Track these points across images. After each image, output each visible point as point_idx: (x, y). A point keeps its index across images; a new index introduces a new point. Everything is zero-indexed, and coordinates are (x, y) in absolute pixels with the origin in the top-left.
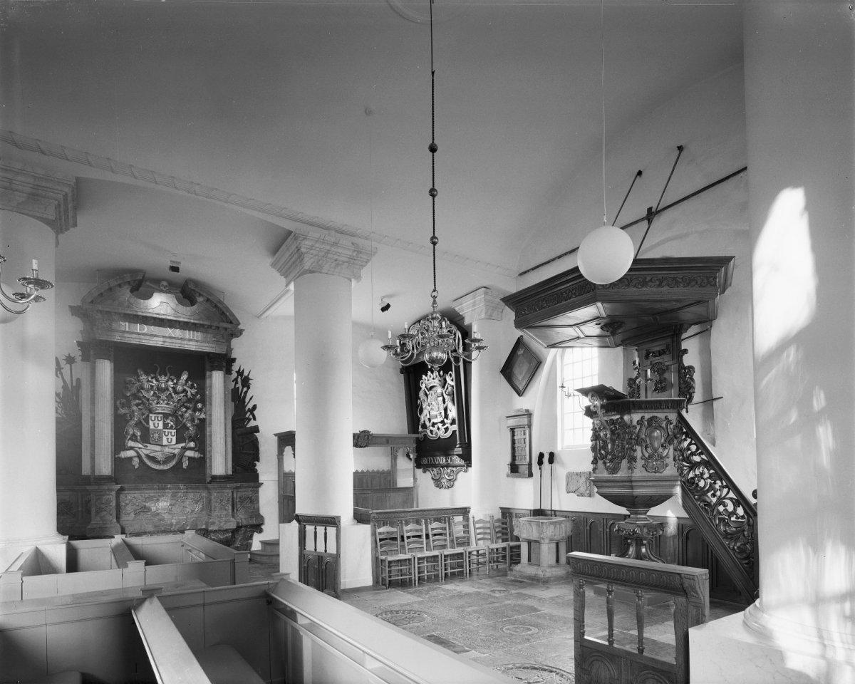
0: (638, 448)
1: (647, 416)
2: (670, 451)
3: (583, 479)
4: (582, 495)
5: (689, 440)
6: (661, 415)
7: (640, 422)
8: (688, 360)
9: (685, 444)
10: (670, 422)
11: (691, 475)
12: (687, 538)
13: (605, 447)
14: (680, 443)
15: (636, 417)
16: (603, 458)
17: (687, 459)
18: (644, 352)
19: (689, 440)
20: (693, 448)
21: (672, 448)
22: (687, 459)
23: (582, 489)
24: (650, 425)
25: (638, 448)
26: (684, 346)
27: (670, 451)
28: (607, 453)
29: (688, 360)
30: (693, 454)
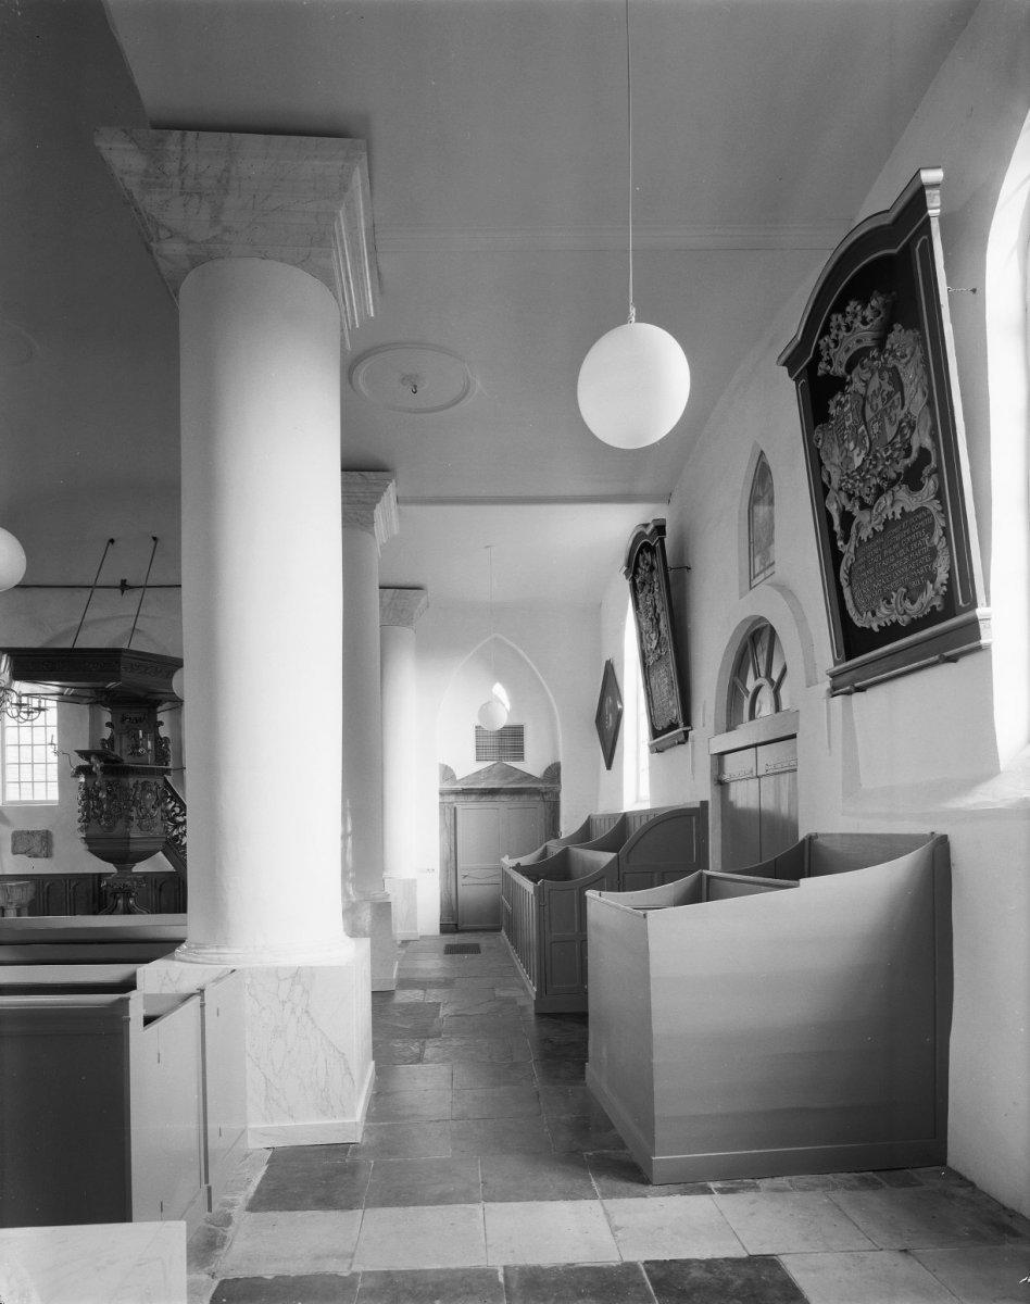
0: (134, 808)
1: (142, 780)
2: (157, 813)
3: (38, 838)
4: (36, 856)
5: (173, 803)
6: (152, 780)
7: (136, 785)
8: (164, 732)
9: (170, 806)
10: (158, 787)
11: (175, 833)
12: (160, 890)
13: (99, 807)
14: (166, 804)
15: (131, 781)
16: (97, 817)
17: (172, 820)
18: (120, 716)
19: (173, 803)
20: (177, 810)
21: (159, 809)
22: (172, 820)
23: (36, 850)
24: (143, 789)
25: (134, 808)
26: (160, 717)
27: (157, 813)
28: (102, 812)
29: (164, 732)
30: (177, 815)
